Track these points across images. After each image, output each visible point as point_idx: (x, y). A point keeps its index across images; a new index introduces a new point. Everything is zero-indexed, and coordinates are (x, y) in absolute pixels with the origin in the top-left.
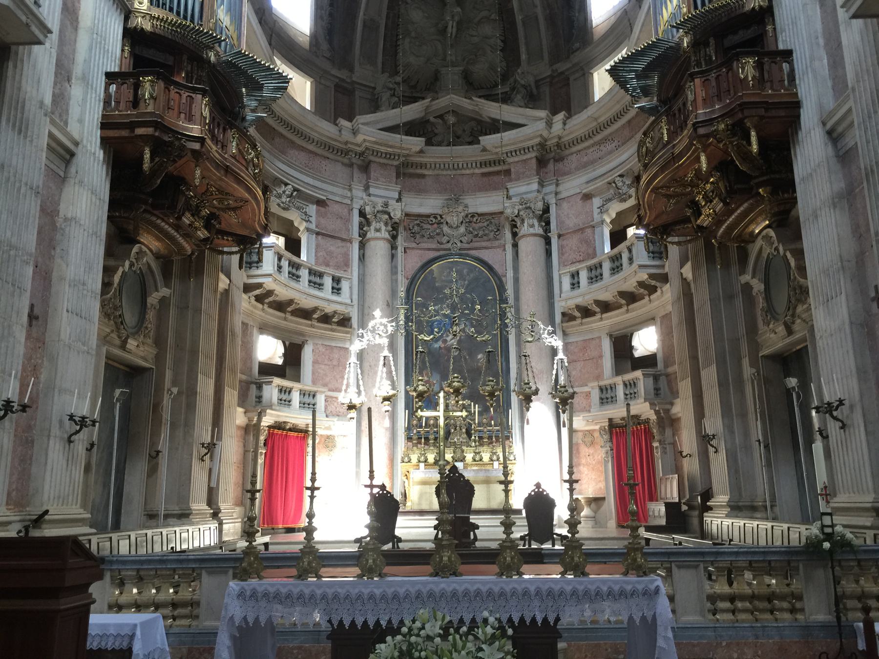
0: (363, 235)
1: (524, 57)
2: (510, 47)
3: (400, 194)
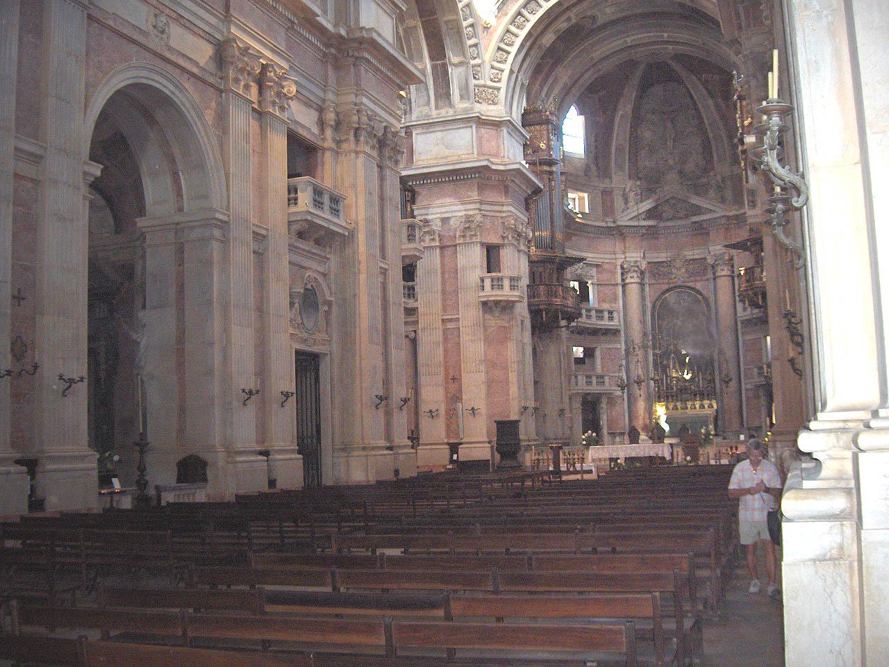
0: (623, 280)
1: (715, 159)
2: (707, 148)
3: (644, 254)
